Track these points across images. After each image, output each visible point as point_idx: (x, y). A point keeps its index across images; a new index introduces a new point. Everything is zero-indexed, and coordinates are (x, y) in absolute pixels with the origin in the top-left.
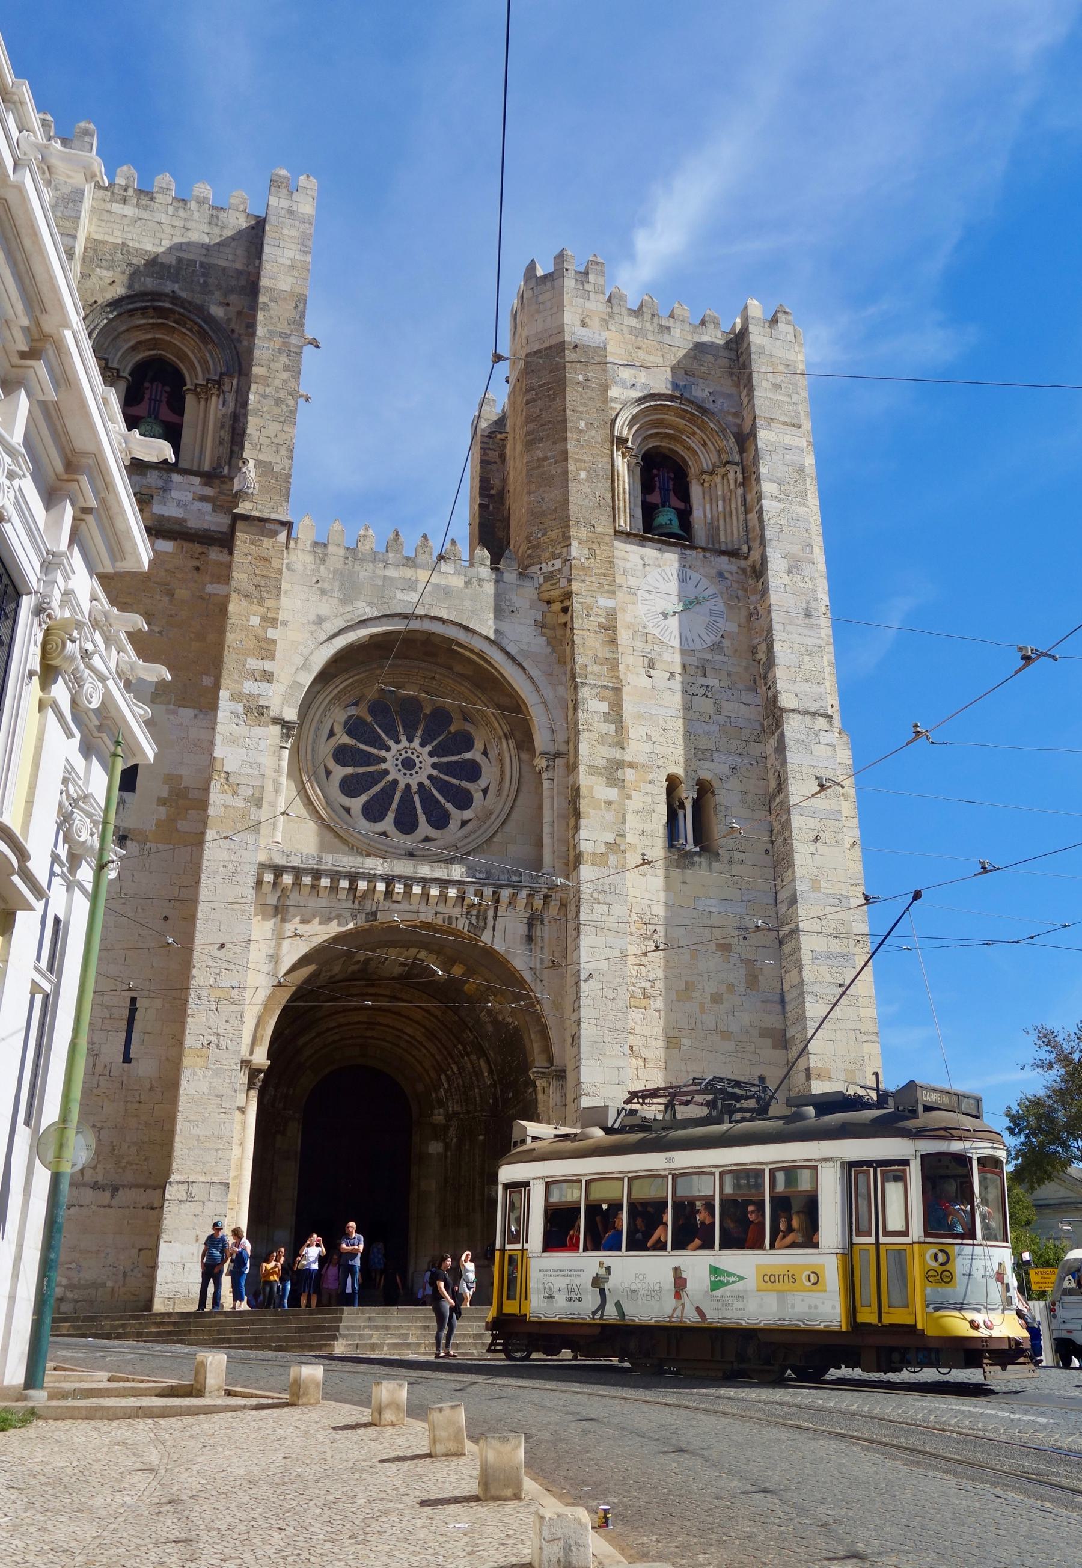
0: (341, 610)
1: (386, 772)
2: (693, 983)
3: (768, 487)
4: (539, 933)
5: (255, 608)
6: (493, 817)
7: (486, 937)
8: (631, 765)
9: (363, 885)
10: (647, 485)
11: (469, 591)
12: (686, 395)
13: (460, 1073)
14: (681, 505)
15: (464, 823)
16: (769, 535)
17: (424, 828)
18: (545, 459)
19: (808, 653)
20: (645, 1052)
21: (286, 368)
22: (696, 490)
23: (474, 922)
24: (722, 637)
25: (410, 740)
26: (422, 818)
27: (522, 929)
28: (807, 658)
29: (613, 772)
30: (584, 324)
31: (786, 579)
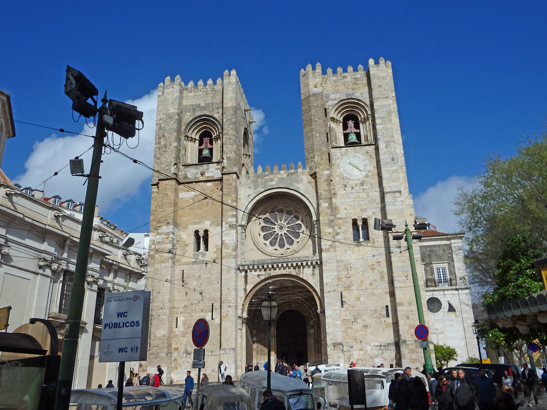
0: (255, 191)
1: (275, 231)
2: (363, 281)
3: (378, 121)
5: (229, 198)
7: (301, 276)
8: (340, 218)
9: (265, 266)
10: (345, 127)
11: (288, 177)
12: (353, 97)
15: (298, 242)
16: (379, 137)
17: (287, 246)
18: (308, 132)
19: (394, 172)
20: (349, 303)
22: (361, 125)
25: (281, 222)
26: (286, 243)
27: (311, 272)
28: (393, 174)
29: (331, 224)
30: (315, 87)
31: (385, 150)
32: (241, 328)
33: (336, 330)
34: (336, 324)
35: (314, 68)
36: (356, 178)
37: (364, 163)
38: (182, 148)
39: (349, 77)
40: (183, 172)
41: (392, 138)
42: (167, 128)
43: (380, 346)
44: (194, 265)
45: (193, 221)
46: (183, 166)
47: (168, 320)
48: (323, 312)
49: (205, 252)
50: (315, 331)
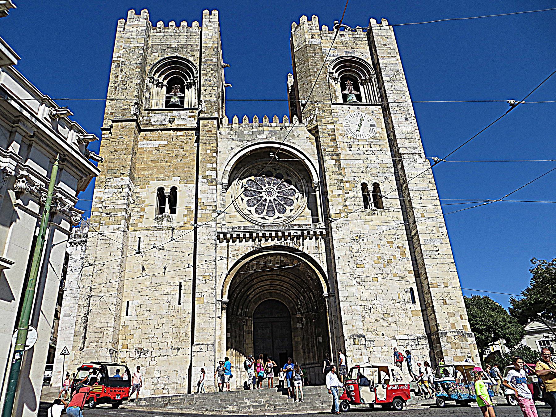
1: (262, 197)
4: (320, 245)
5: (208, 147)
6: (300, 207)
7: (300, 248)
12: (353, 55)
13: (304, 299)
14: (356, 93)
19: (408, 133)
20: (364, 284)
21: (212, 70)
23: (296, 243)
24: (376, 133)
27: (314, 244)
28: (408, 135)
30: (312, 38)
31: (397, 109)
32: (220, 315)
33: (354, 318)
34: (355, 310)
35: (310, 19)
36: (363, 139)
37: (370, 123)
38: (145, 90)
39: (347, 36)
40: (145, 118)
41: (404, 97)
42: (128, 63)
43: (408, 339)
44: (155, 232)
45: (156, 176)
46: (145, 110)
47: (115, 303)
48: (334, 294)
49: (171, 215)
50: (303, 325)
